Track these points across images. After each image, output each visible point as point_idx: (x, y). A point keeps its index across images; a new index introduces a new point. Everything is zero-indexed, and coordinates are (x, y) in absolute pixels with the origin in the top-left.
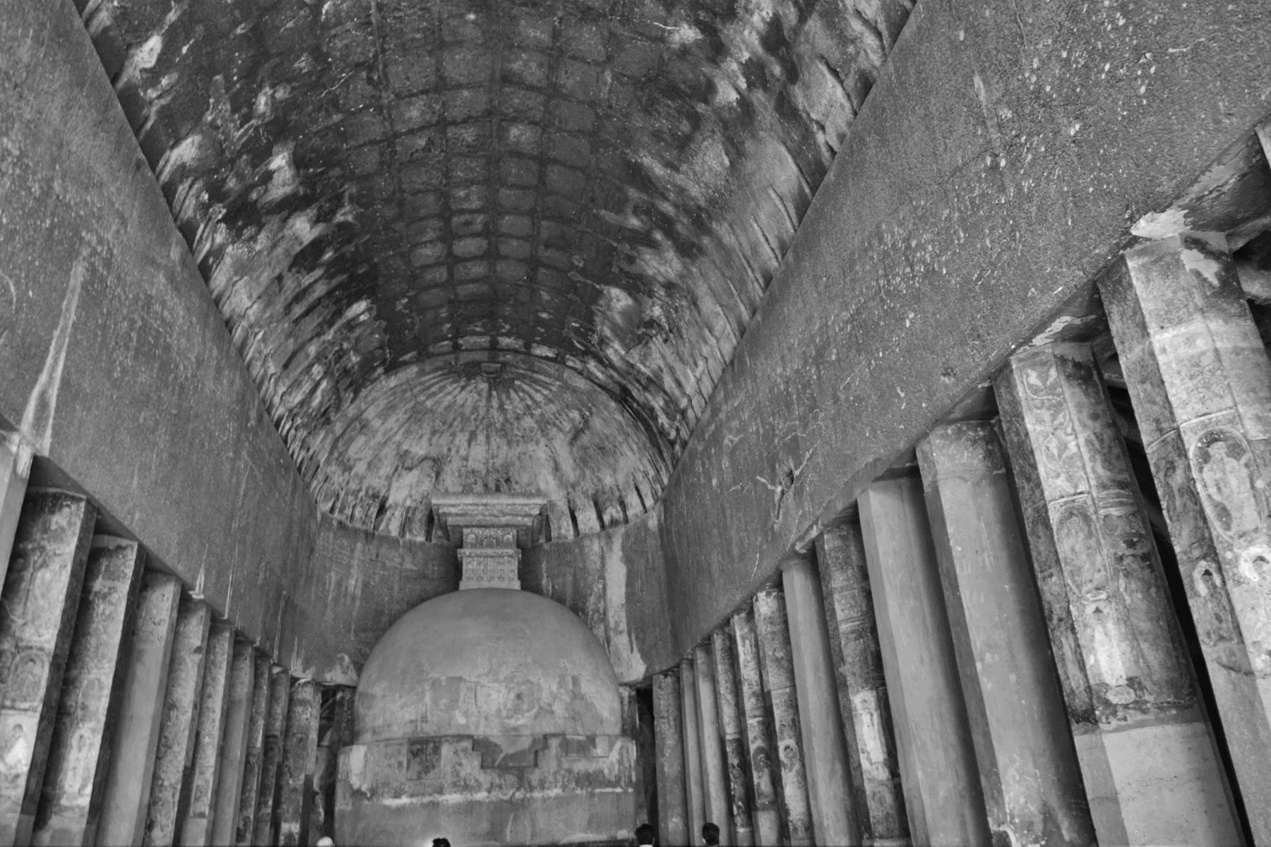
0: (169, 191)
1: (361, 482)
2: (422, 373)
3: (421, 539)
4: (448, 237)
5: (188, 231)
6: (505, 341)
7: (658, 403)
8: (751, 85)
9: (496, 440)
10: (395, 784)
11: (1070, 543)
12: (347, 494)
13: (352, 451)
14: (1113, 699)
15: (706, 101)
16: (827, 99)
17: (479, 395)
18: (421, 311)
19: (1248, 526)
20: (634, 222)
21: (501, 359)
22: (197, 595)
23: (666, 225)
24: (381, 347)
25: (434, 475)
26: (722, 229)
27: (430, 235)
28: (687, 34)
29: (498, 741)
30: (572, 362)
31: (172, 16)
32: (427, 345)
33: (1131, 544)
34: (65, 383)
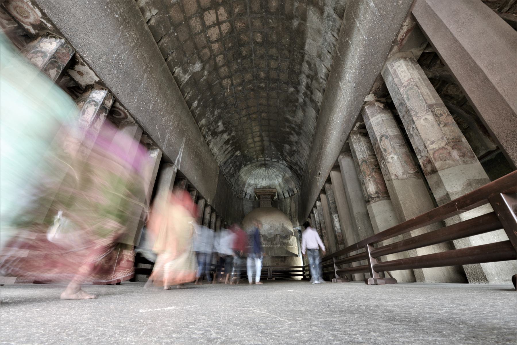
0: (200, 129)
2: (252, 166)
4: (253, 137)
5: (204, 136)
6: (267, 159)
7: (297, 168)
8: (305, 97)
9: (267, 180)
11: (363, 167)
14: (373, 196)
15: (297, 102)
16: (318, 96)
18: (250, 153)
19: (390, 151)
20: (288, 130)
22: (209, 202)
23: (294, 129)
26: (303, 128)
27: (249, 137)
28: (292, 89)
30: (280, 162)
31: (199, 97)
33: (376, 166)
34: (182, 158)
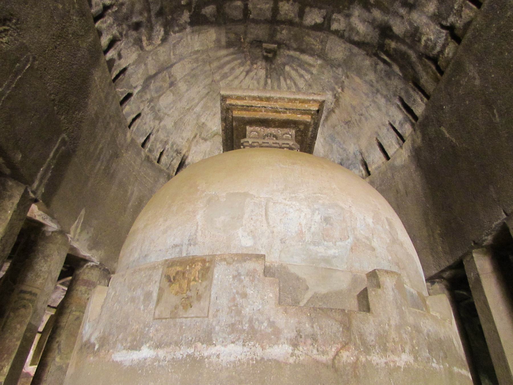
10: (136, 326)
17: (258, 83)
29: (301, 274)
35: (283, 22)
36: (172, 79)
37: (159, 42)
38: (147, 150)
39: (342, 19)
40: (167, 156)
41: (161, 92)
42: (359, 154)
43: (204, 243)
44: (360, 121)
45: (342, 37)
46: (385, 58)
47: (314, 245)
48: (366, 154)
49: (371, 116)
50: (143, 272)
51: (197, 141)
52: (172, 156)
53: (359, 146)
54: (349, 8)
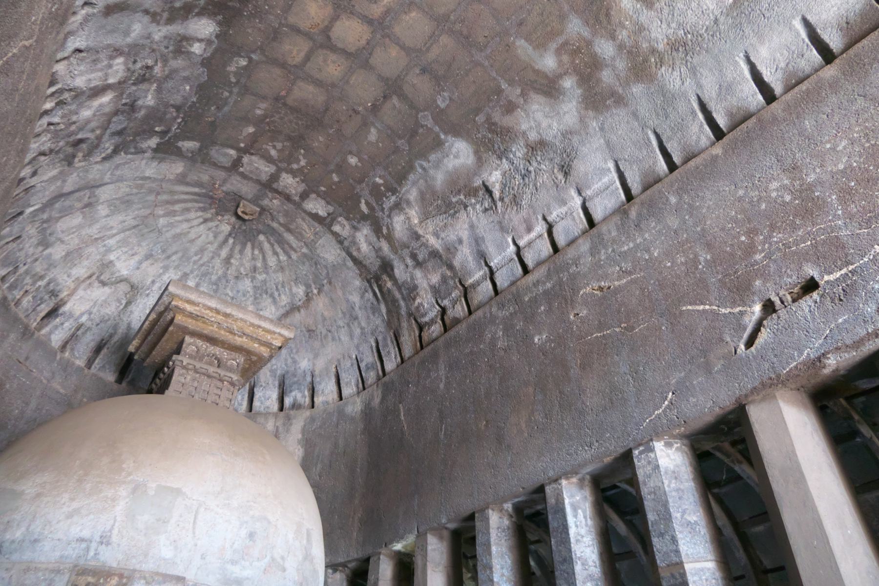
1: (48, 269)
2: (182, 179)
3: (80, 363)
12: (27, 272)
13: (61, 225)
17: (215, 237)
21: (266, 202)
24: (178, 108)
25: (124, 302)
30: (342, 227)
32: (214, 143)
35: (276, 191)
36: (93, 200)
37: (99, 159)
38: (7, 285)
39: (348, 227)
40: (34, 297)
41: (66, 212)
42: (309, 373)
43: (119, 545)
44: (326, 337)
45: (341, 242)
46: (377, 291)
47: (232, 564)
48: (318, 379)
49: (340, 339)
50: (40, 574)
51: (90, 284)
52: (41, 299)
53: (314, 365)
54: (359, 222)
